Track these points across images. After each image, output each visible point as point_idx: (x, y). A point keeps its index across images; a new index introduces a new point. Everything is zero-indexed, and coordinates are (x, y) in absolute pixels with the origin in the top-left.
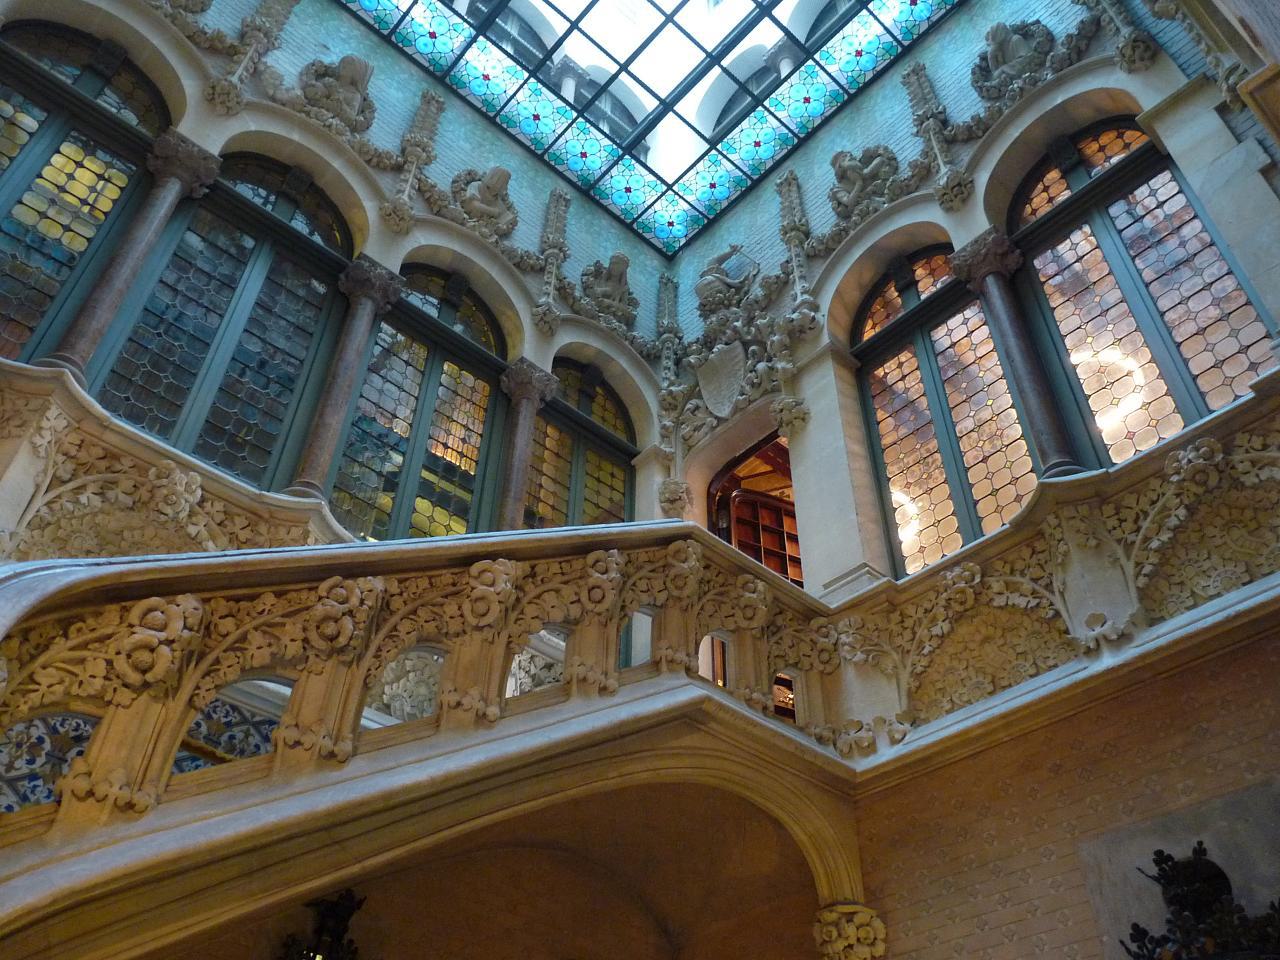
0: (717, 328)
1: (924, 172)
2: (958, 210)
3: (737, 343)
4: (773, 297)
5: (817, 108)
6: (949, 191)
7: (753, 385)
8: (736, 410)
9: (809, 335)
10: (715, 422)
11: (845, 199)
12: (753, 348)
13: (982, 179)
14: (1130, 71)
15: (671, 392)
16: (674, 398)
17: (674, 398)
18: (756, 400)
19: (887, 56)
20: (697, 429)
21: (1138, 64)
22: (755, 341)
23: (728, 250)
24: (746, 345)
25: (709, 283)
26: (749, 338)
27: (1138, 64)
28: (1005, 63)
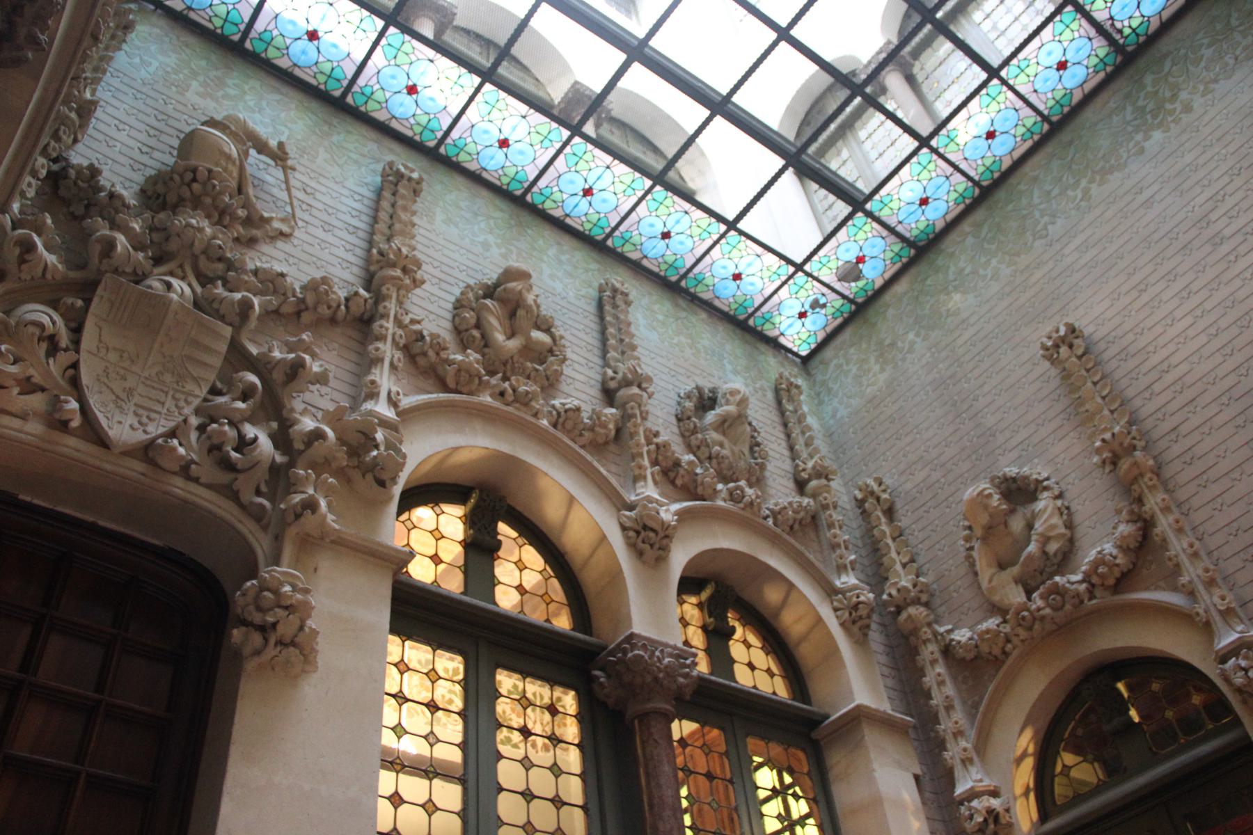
0: (198, 247)
1: (601, 440)
2: (644, 563)
3: (227, 331)
4: (306, 317)
5: (492, 162)
6: (661, 534)
7: (215, 449)
8: (147, 452)
9: (366, 485)
10: (75, 423)
11: (500, 337)
12: (252, 378)
13: (680, 558)
14: (842, 625)
15: (29, 247)
16: (22, 261)
17: (22, 261)
18: (196, 480)
19: (663, 267)
20: (29, 387)
21: (855, 629)
22: (258, 365)
23: (273, 143)
24: (238, 357)
25: (229, 157)
26: (254, 350)
27: (855, 629)
28: (724, 434)
